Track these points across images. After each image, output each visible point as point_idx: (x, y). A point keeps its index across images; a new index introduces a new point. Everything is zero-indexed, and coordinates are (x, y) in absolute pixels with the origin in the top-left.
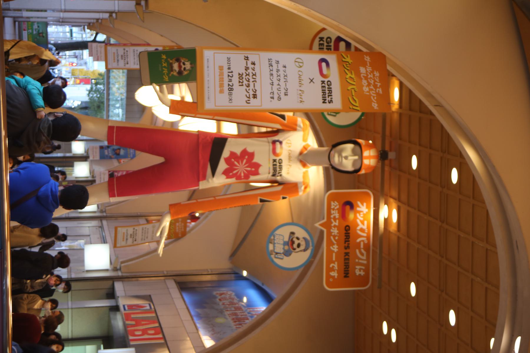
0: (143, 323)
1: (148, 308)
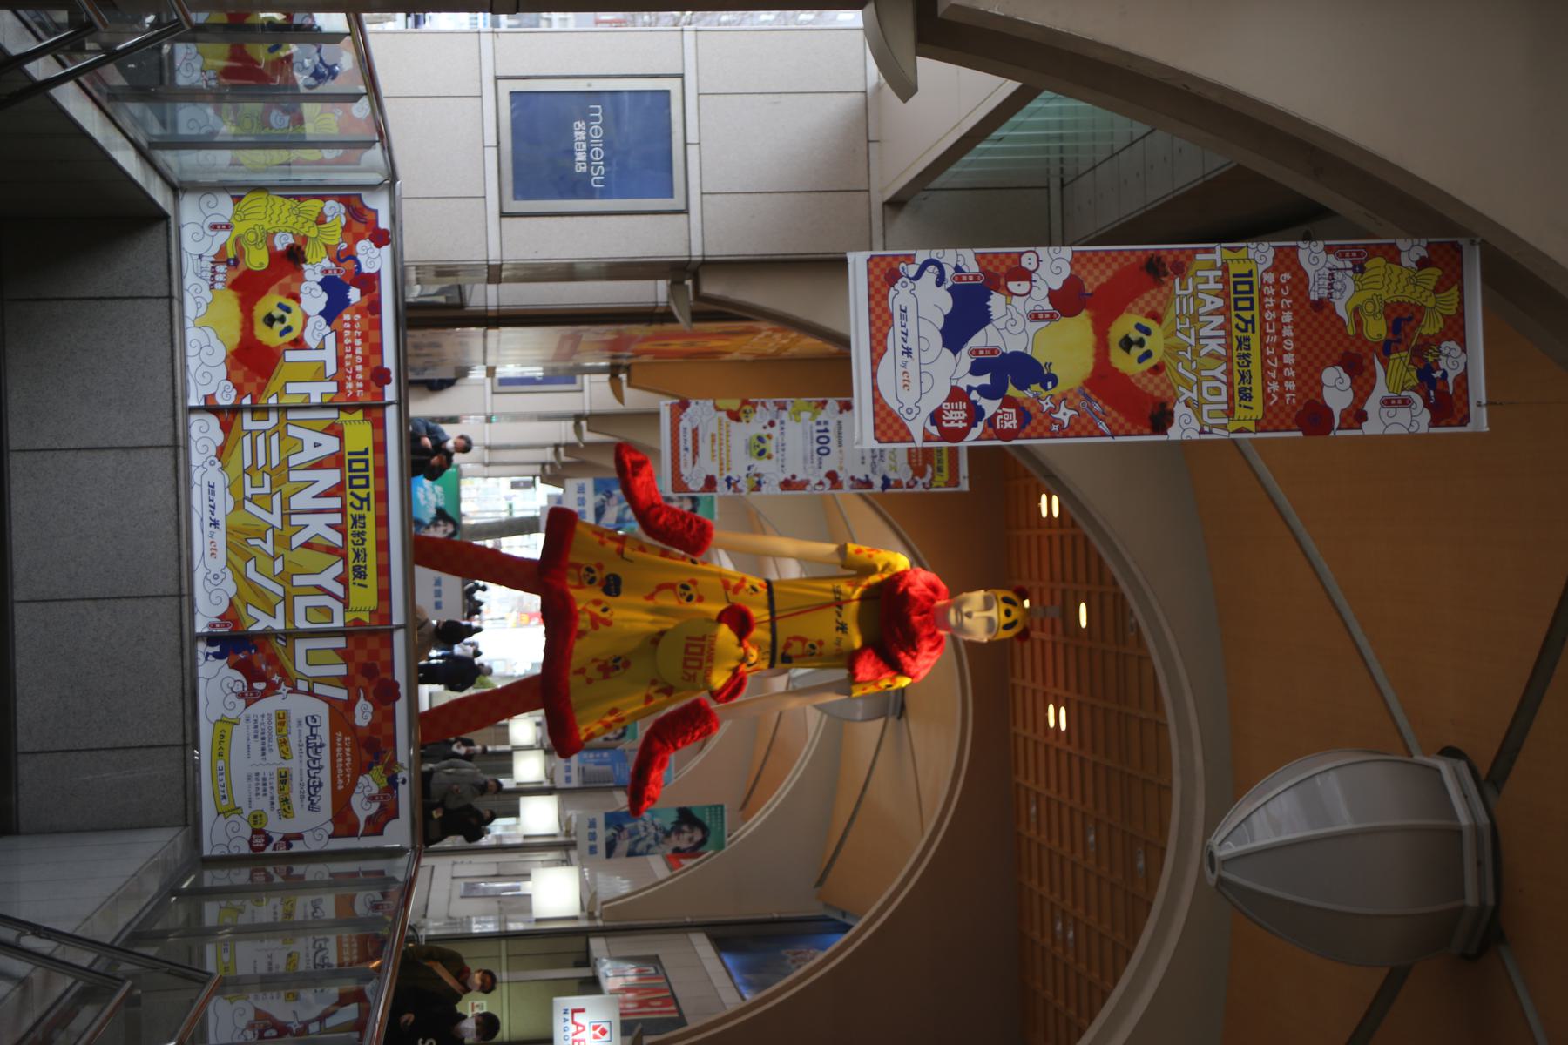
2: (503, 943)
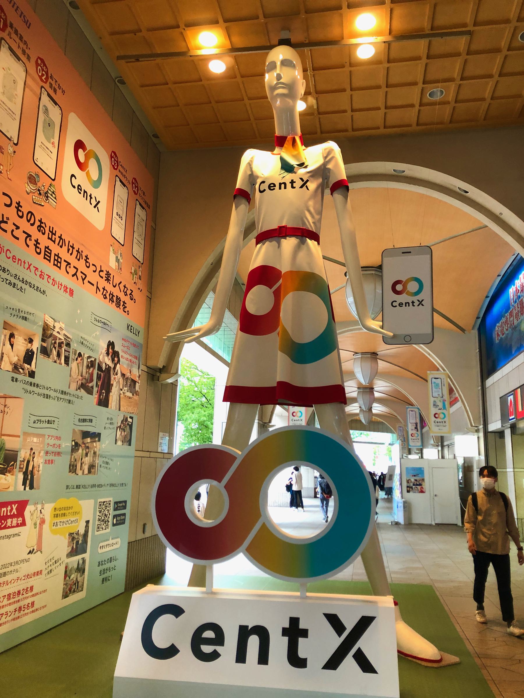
1: (512, 397)
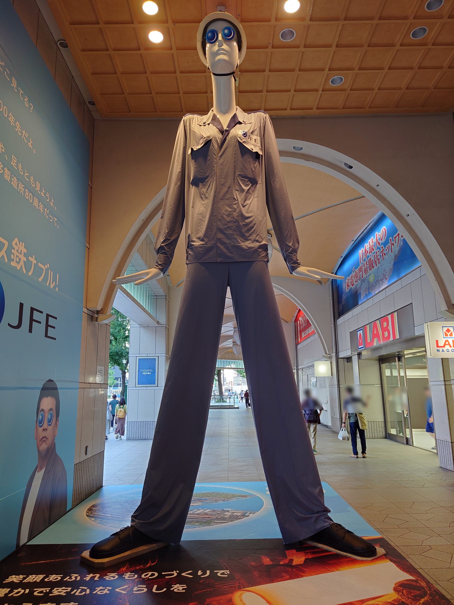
0: (375, 332)
1: (361, 331)
2: (341, 386)
